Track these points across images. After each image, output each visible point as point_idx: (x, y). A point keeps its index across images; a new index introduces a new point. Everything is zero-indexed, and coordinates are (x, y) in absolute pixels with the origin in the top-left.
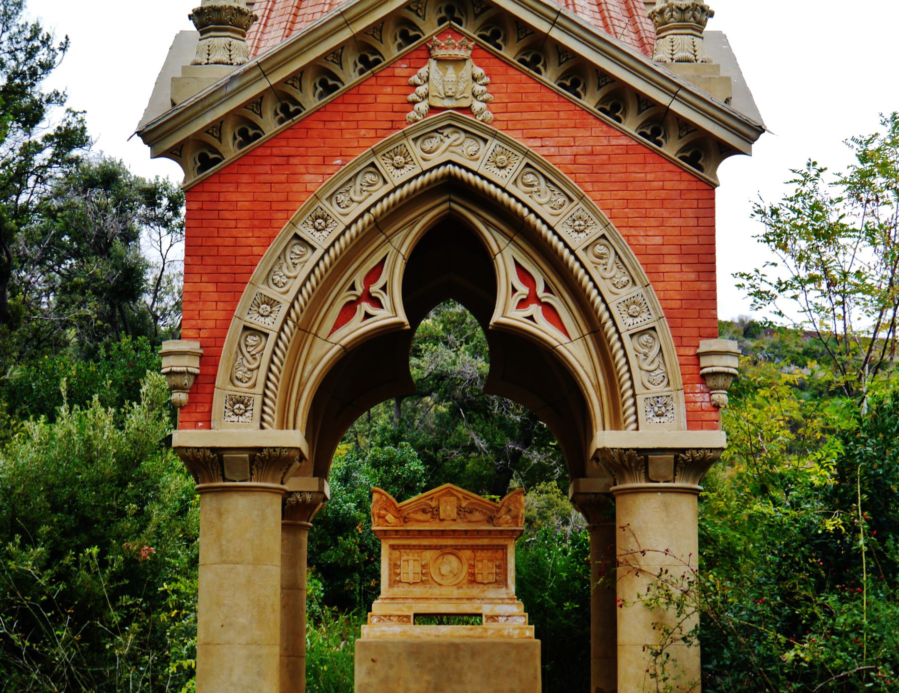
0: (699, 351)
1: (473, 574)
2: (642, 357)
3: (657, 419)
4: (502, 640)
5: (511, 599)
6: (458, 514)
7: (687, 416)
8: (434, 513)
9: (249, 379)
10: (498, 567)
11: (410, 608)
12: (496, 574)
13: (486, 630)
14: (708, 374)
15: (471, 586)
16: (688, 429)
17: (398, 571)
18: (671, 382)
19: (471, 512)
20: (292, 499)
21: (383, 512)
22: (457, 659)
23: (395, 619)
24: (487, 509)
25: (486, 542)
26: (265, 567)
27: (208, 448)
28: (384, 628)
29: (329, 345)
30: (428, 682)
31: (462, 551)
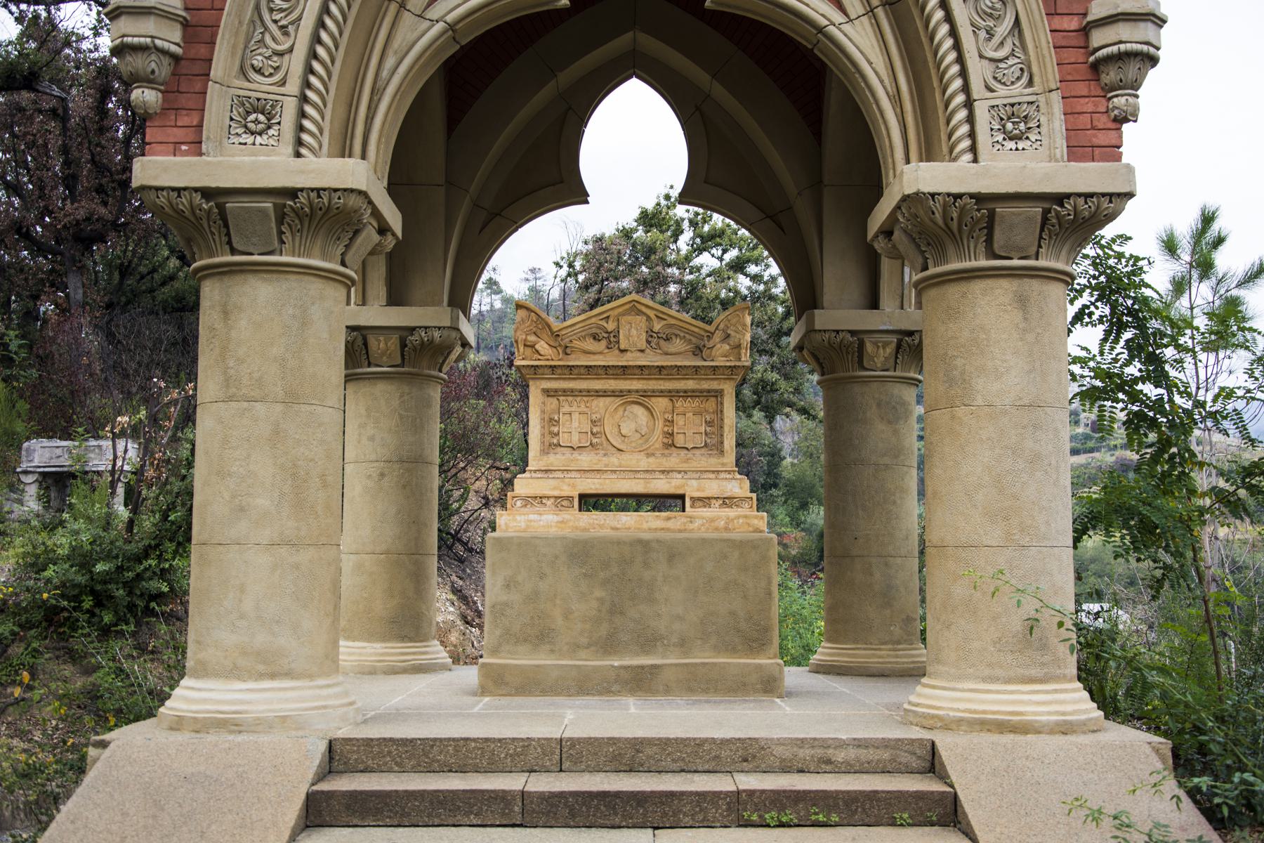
0: (1089, 18)
1: (672, 435)
2: (983, 34)
3: (1012, 145)
4: (715, 535)
5: (729, 472)
6: (648, 342)
7: (1068, 139)
8: (612, 339)
9: (277, 69)
10: (709, 423)
11: (574, 486)
12: (706, 434)
13: (692, 519)
14: (1109, 59)
15: (666, 452)
16: (1069, 160)
17: (556, 429)
18: (1036, 79)
19: (667, 339)
20: (414, 338)
21: (532, 338)
22: (646, 565)
23: (549, 503)
24: (692, 333)
25: (690, 385)
26: (308, 408)
27: (196, 190)
28: (532, 517)
29: (427, 24)
30: (601, 601)
31: (653, 399)
